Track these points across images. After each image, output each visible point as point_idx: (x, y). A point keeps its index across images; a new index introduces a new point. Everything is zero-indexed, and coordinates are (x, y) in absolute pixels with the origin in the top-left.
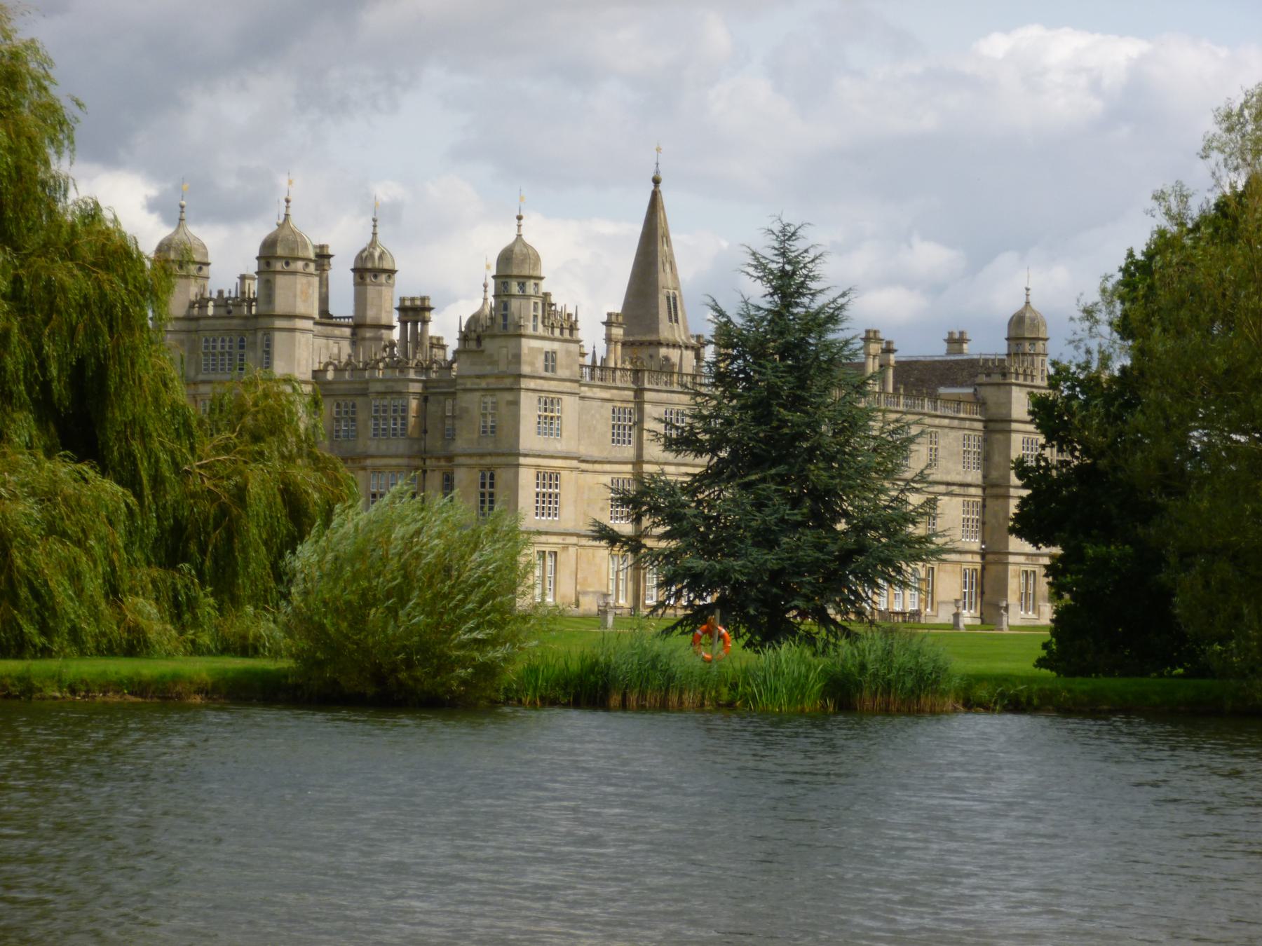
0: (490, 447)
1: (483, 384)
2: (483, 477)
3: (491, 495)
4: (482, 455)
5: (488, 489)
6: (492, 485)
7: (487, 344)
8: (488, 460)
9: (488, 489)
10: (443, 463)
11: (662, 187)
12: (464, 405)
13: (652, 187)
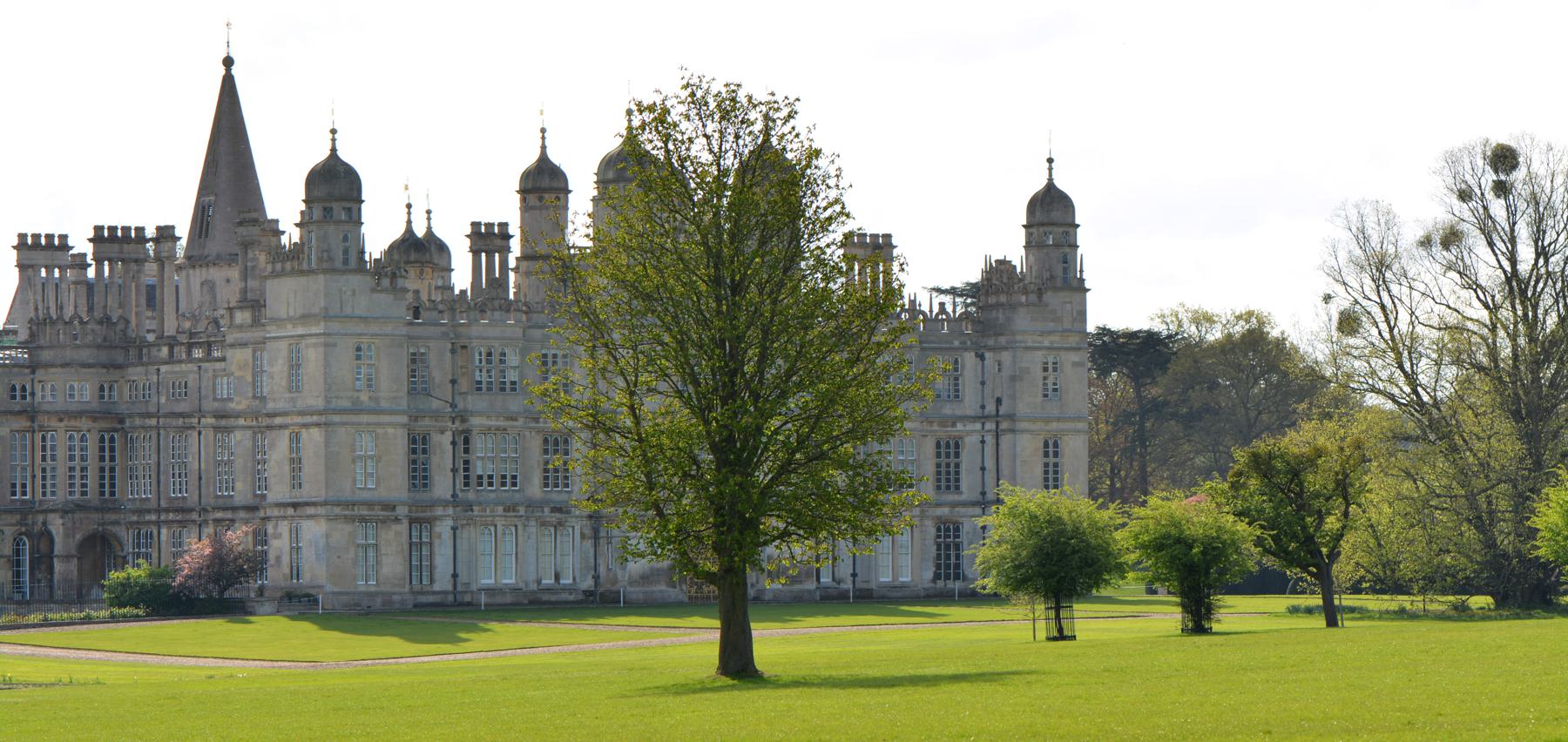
0: (1056, 412)
1: (1047, 343)
2: (1046, 445)
3: (1056, 465)
4: (1048, 420)
5: (1052, 460)
6: (1056, 454)
7: (1049, 297)
8: (1054, 425)
9: (1052, 460)
10: (935, 427)
11: (235, 71)
12: (1024, 365)
13: (222, 70)
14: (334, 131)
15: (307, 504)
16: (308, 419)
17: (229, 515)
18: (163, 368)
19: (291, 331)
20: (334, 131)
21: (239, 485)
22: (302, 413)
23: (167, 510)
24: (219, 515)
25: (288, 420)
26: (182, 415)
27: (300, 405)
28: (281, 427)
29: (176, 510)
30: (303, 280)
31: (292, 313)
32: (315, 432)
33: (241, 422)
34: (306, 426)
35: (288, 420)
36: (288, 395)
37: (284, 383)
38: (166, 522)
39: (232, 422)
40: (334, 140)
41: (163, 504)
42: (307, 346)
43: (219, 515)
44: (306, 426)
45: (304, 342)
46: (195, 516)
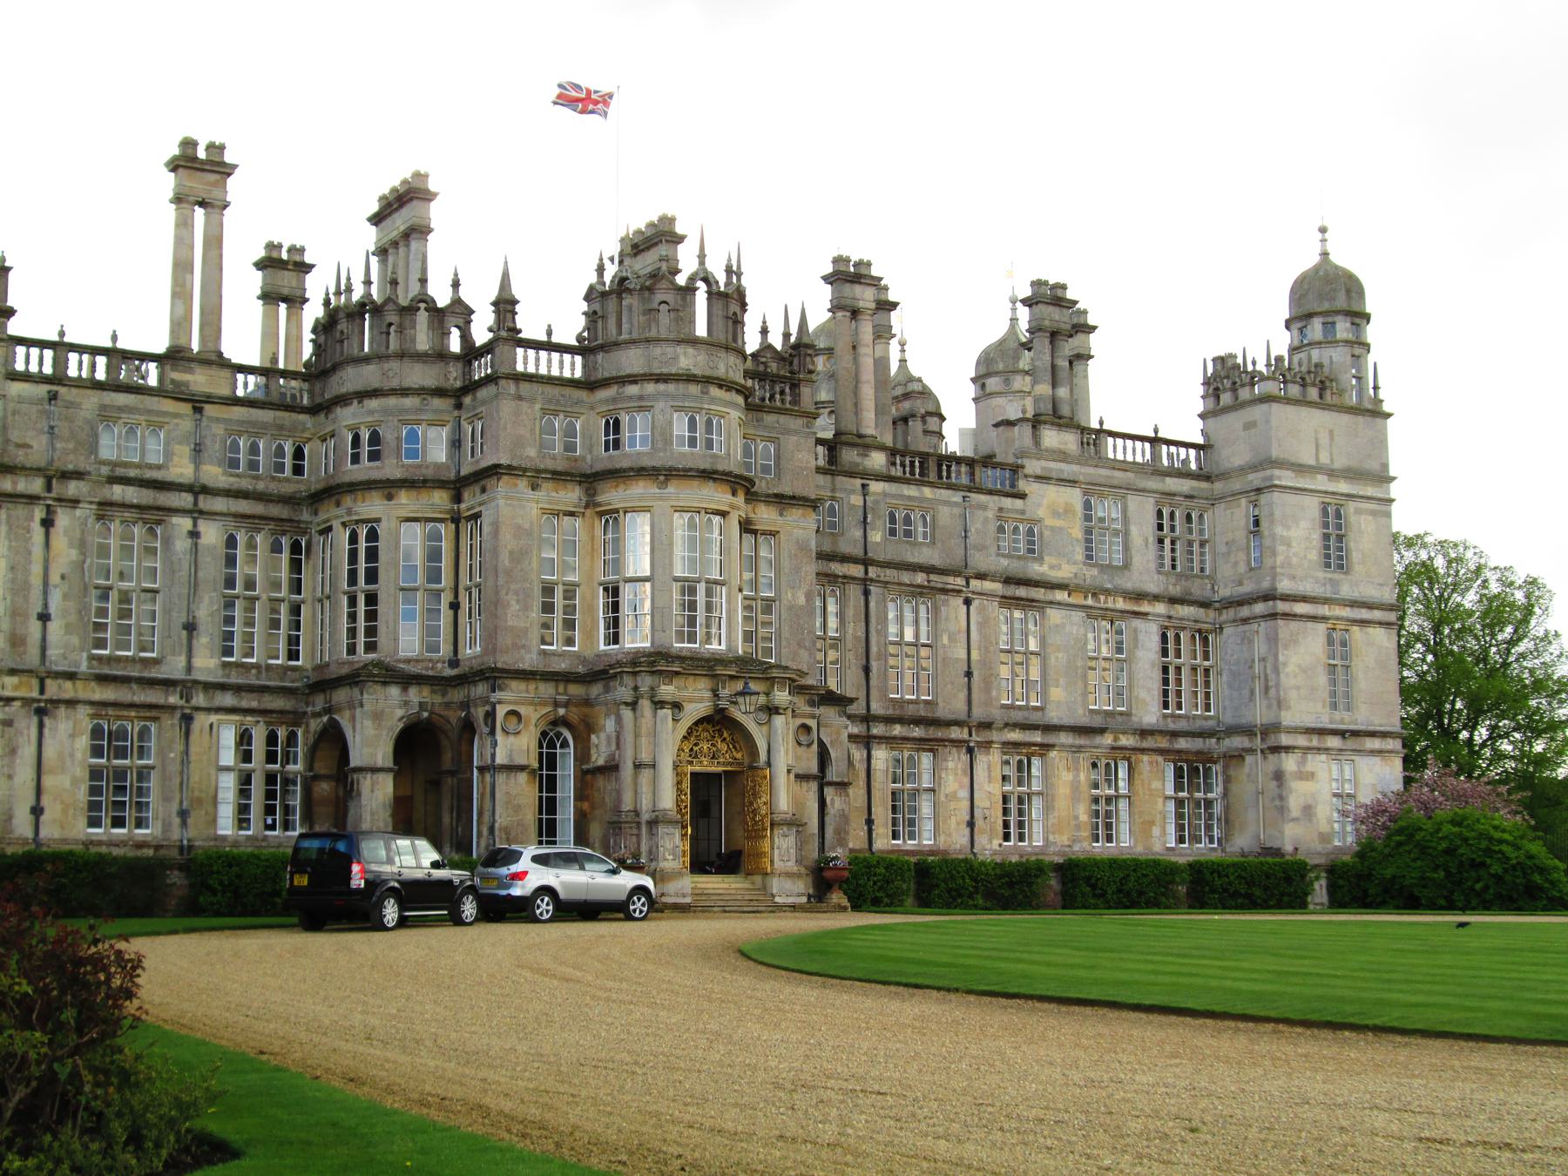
14: (1323, 230)
15: (1372, 734)
16: (1364, 614)
17: (1037, 737)
18: (876, 487)
19: (1321, 482)
20: (1323, 230)
21: (1056, 693)
22: (1354, 604)
23: (889, 720)
24: (1015, 736)
25: (1324, 610)
26: (929, 570)
27: (1346, 591)
28: (1324, 619)
29: (917, 721)
30: (1345, 419)
31: (1324, 459)
32: (1379, 634)
33: (1061, 596)
34: (1363, 623)
35: (1324, 610)
36: (1321, 574)
37: (1314, 555)
38: (889, 741)
39: (1038, 594)
40: (1323, 241)
41: (877, 708)
42: (1358, 512)
43: (1015, 736)
44: (1363, 623)
45: (1351, 506)
46: (956, 733)
